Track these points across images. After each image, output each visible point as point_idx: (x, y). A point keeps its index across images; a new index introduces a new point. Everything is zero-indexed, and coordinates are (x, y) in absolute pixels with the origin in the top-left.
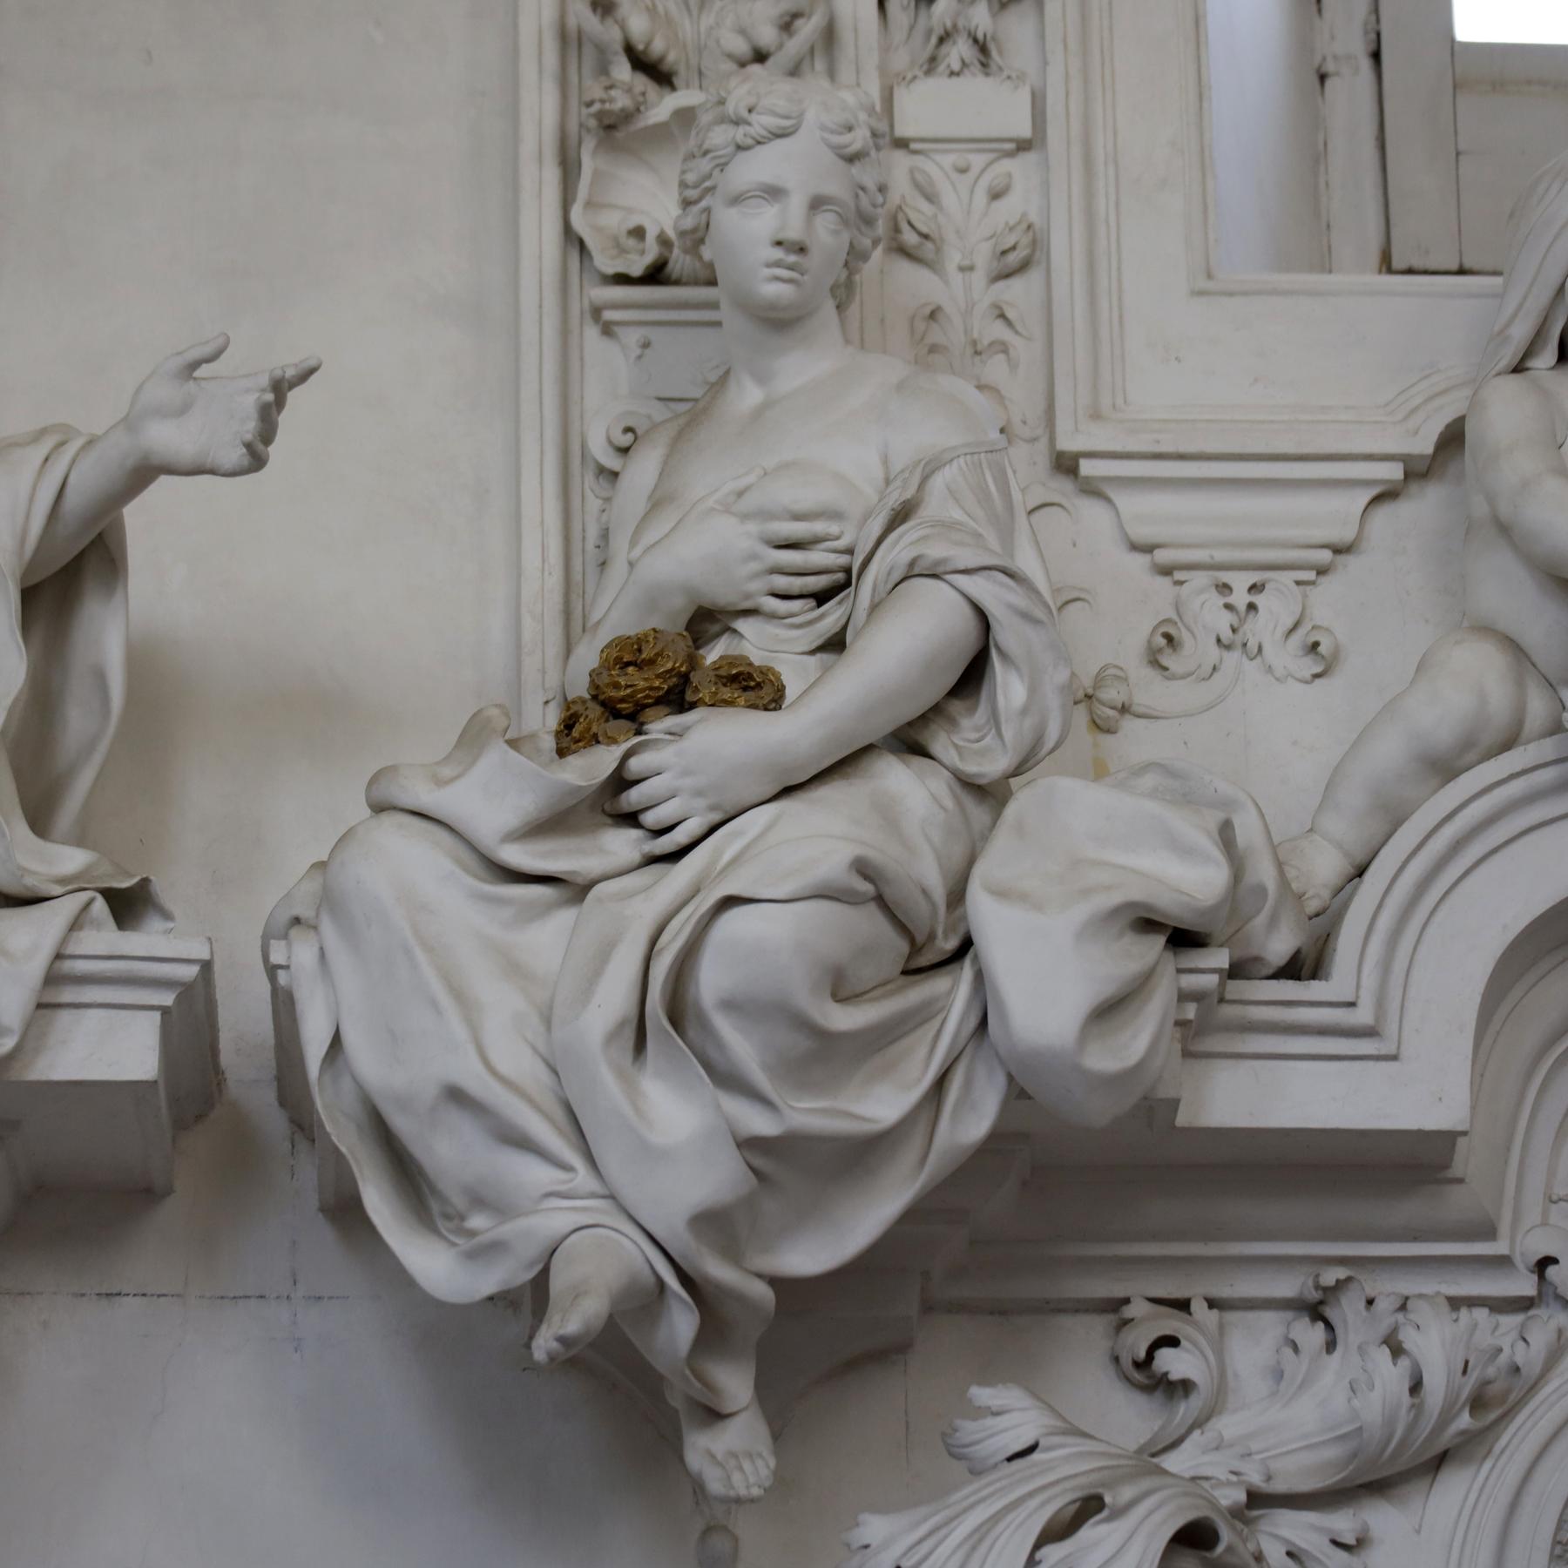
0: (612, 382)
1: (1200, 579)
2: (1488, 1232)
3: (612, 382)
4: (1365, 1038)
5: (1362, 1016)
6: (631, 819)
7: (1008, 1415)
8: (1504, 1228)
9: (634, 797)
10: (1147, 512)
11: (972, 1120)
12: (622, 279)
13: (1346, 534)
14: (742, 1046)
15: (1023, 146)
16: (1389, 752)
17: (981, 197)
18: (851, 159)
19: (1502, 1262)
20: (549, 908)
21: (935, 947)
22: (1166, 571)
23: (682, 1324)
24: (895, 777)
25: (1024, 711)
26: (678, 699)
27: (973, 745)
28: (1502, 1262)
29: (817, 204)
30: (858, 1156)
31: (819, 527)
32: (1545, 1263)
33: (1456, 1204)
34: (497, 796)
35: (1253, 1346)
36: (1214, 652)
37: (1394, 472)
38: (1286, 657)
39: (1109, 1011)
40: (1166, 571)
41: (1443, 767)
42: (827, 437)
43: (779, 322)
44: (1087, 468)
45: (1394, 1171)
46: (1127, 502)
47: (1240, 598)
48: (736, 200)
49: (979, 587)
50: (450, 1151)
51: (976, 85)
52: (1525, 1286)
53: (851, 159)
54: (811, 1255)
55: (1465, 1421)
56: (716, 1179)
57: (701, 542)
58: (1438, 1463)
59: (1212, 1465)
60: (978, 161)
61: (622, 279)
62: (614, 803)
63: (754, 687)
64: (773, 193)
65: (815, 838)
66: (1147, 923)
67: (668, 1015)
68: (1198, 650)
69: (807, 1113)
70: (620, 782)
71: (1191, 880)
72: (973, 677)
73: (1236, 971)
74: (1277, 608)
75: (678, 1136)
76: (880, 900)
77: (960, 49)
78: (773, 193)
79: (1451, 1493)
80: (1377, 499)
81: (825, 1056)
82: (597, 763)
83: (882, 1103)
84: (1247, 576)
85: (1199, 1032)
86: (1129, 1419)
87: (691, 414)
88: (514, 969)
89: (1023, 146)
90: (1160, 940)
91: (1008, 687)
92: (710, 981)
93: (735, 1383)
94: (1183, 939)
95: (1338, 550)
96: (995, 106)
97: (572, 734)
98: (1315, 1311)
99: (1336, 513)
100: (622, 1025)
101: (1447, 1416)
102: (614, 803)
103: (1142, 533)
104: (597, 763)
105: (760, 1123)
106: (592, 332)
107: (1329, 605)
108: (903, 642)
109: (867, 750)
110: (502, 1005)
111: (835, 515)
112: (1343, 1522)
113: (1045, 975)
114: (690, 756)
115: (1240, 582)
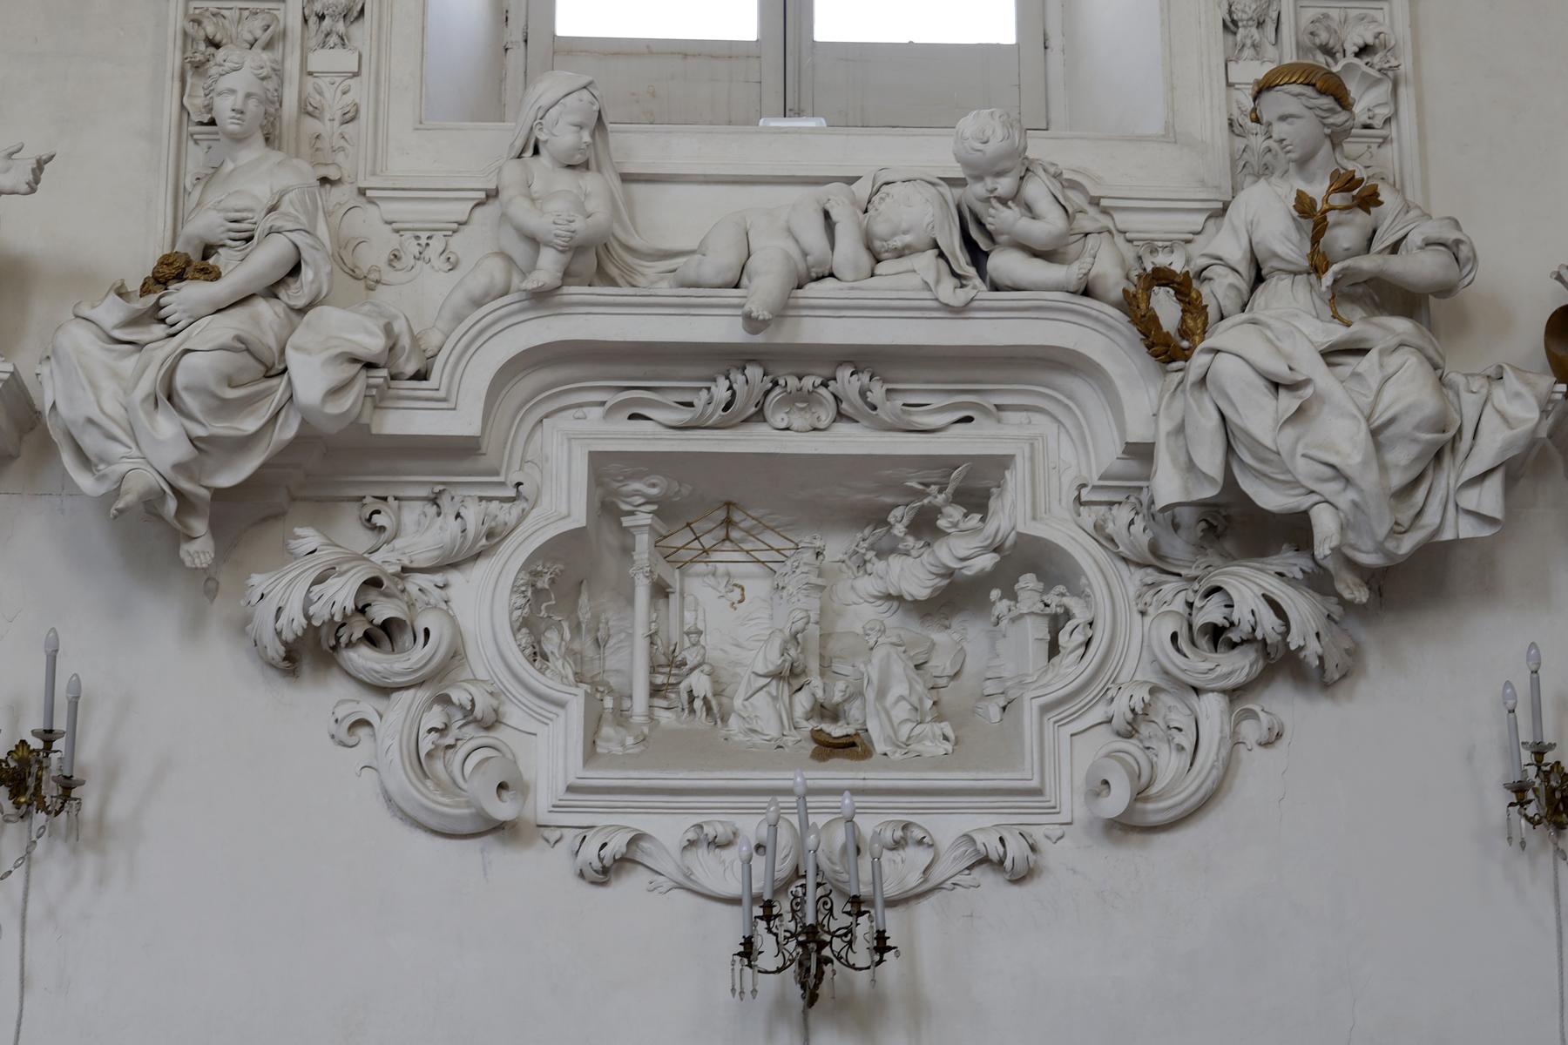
0: (196, 158)
1: (408, 234)
2: (497, 474)
3: (196, 158)
4: (444, 401)
5: (442, 394)
6: (163, 321)
7: (308, 538)
8: (503, 471)
9: (163, 313)
10: (391, 209)
11: (288, 431)
12: (201, 124)
13: (464, 218)
14: (191, 402)
15: (356, 75)
16: (459, 298)
17: (339, 93)
18: (263, 79)
19: (502, 484)
20: (132, 353)
21: (275, 370)
22: (397, 231)
23: (172, 504)
24: (262, 307)
25: (313, 282)
26: (180, 277)
27: (297, 294)
28: (502, 484)
29: (248, 96)
30: (244, 444)
31: (244, 215)
32: (519, 484)
33: (483, 463)
34: (111, 312)
35: (412, 514)
36: (412, 261)
37: (482, 195)
38: (439, 263)
39: (336, 391)
40: (397, 231)
41: (478, 303)
42: (257, 180)
43: (238, 139)
44: (368, 193)
45: (460, 450)
46: (384, 206)
47: (423, 241)
48: (220, 94)
49: (296, 237)
50: (91, 442)
51: (339, 51)
52: (512, 493)
53: (263, 79)
54: (226, 480)
55: (484, 541)
56: (184, 451)
57: (206, 223)
58: (478, 556)
59: (387, 560)
60: (339, 80)
61: (201, 124)
62: (156, 315)
63: (212, 274)
64: (233, 91)
65: (225, 327)
66: (355, 360)
67: (169, 394)
68: (407, 260)
69: (220, 428)
70: (158, 307)
71: (373, 344)
72: (295, 270)
73: (393, 377)
74: (437, 244)
75: (167, 437)
76: (248, 350)
77: (333, 39)
78: (233, 91)
79: (481, 569)
80: (477, 205)
81: (225, 408)
82: (151, 299)
83: (250, 425)
84: (424, 234)
85: (378, 400)
86: (362, 540)
87: (210, 176)
88: (115, 375)
89: (356, 75)
90: (359, 366)
91: (307, 273)
92: (180, 380)
93: (200, 526)
94: (370, 366)
95: (460, 224)
96: (344, 60)
97: (145, 290)
98: (434, 500)
99: (461, 210)
100: (148, 396)
101: (476, 540)
102: (156, 315)
103: (389, 217)
104: (151, 299)
105: (199, 431)
106: (191, 143)
107: (456, 243)
108: (266, 257)
109: (253, 296)
110: (108, 388)
111: (251, 210)
112: (439, 578)
113: (310, 378)
114: (186, 296)
115: (424, 235)
